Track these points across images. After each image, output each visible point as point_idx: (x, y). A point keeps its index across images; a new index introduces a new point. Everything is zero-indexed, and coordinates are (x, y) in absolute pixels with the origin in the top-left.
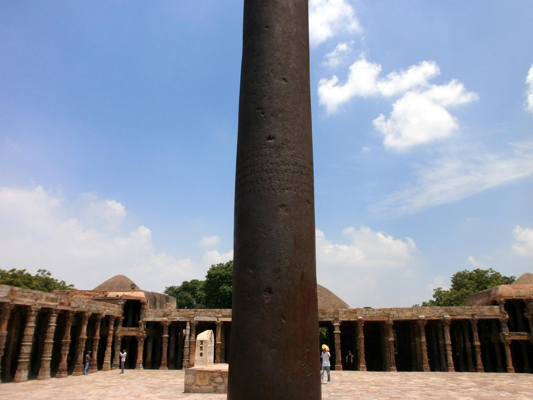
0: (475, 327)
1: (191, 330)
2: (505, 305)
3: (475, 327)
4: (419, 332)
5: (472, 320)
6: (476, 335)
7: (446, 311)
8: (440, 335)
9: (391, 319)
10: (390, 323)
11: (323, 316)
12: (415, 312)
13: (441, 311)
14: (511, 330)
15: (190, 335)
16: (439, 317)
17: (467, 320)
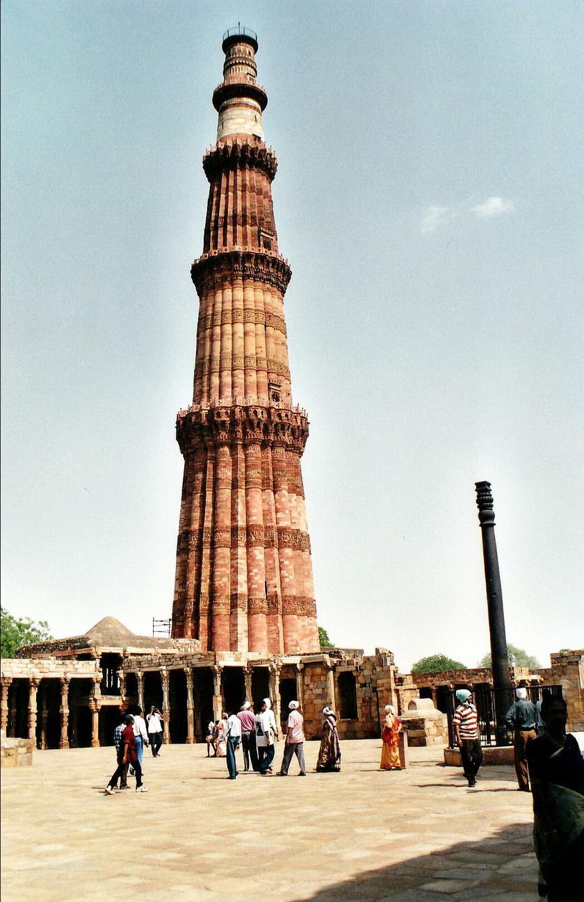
6: (65, 699)
17: (57, 680)
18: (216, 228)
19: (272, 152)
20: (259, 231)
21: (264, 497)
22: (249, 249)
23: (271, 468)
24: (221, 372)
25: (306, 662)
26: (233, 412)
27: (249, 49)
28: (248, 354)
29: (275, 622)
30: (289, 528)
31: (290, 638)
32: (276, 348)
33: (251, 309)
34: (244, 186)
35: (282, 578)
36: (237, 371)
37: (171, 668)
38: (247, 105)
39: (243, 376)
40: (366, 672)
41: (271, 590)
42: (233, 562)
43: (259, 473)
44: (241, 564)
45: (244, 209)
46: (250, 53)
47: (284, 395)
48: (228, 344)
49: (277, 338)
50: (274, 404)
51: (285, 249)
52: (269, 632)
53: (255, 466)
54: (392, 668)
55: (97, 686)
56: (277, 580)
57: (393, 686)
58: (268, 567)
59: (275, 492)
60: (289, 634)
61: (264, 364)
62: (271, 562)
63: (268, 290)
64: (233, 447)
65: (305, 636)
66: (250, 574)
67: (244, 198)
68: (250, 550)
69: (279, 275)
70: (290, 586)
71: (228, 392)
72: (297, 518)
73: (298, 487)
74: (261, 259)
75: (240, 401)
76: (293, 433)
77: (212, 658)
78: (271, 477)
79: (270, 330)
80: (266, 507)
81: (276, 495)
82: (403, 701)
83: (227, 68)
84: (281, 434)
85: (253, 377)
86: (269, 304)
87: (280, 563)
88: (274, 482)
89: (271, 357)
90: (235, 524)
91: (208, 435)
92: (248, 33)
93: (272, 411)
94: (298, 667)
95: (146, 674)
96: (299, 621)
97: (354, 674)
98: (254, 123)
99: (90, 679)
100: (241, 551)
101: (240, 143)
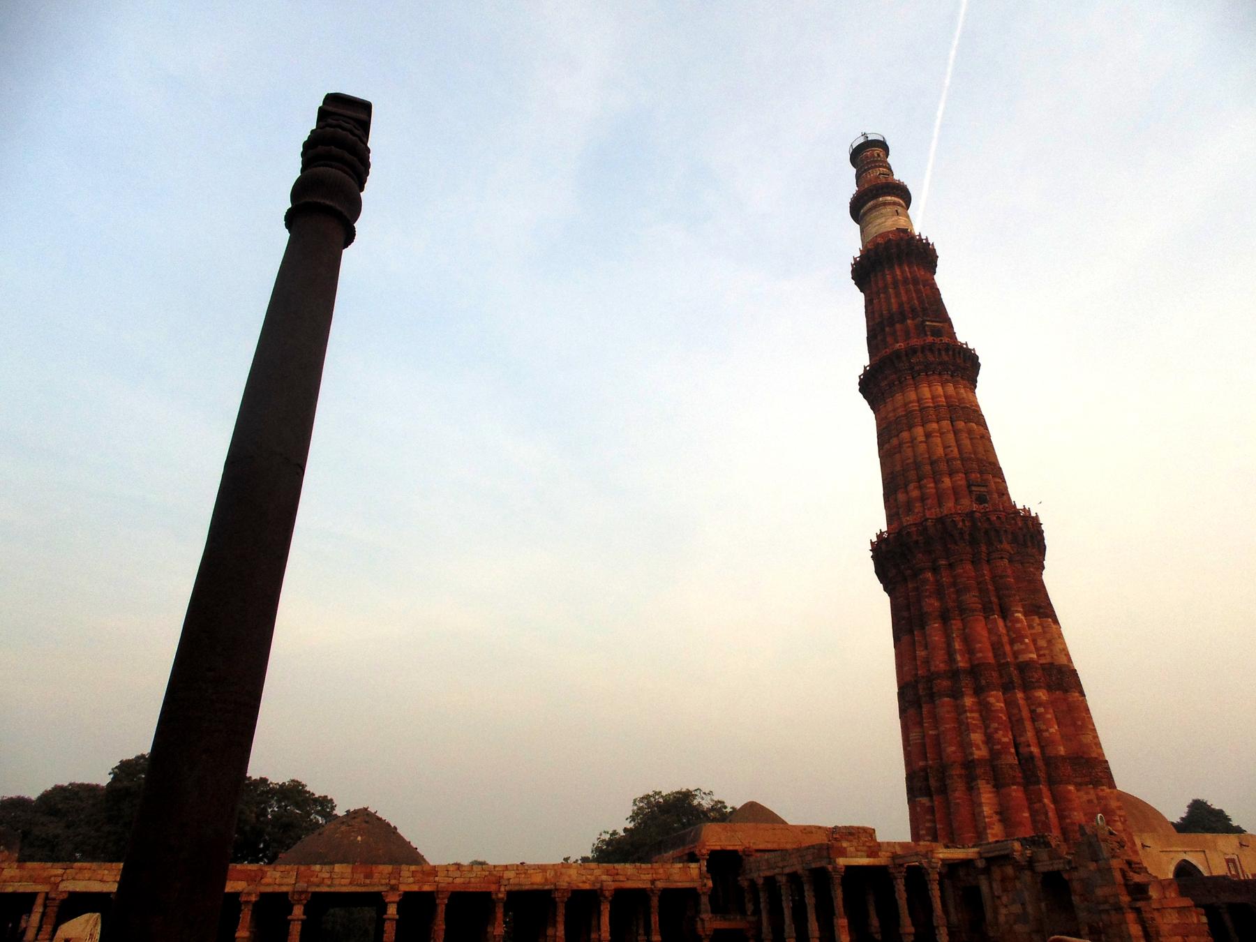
0: (655, 902)
1: (44, 914)
2: (708, 861)
3: (655, 902)
4: (555, 915)
5: (652, 890)
6: (655, 919)
7: (608, 873)
8: (594, 923)
9: (502, 889)
10: (500, 896)
11: (368, 881)
12: (550, 874)
13: (597, 872)
14: (715, 910)
15: (40, 929)
16: (593, 883)
19: (923, 237)
24: (906, 486)
25: (986, 855)
26: (926, 529)
27: (878, 150)
28: (935, 458)
32: (973, 445)
34: (895, 284)
35: (1038, 732)
37: (787, 870)
38: (885, 204)
39: (932, 485)
40: (1082, 873)
41: (1023, 750)
42: (963, 717)
44: (973, 718)
45: (901, 305)
47: (995, 496)
48: (908, 452)
49: (970, 432)
51: (964, 334)
52: (1033, 813)
54: (1115, 863)
55: (704, 900)
56: (1030, 734)
57: (1125, 899)
59: (1004, 618)
62: (1015, 711)
64: (935, 570)
67: (897, 295)
69: (965, 365)
71: (918, 506)
72: (1046, 648)
73: (1040, 607)
74: (931, 348)
77: (825, 853)
78: (994, 599)
79: (961, 425)
80: (994, 638)
82: (1158, 933)
83: (858, 177)
85: (947, 482)
86: (951, 397)
87: (1032, 712)
88: (1000, 606)
93: (977, 515)
94: (980, 864)
95: (766, 878)
96: (1079, 794)
97: (1065, 876)
99: (694, 889)
100: (968, 701)
101: (880, 240)
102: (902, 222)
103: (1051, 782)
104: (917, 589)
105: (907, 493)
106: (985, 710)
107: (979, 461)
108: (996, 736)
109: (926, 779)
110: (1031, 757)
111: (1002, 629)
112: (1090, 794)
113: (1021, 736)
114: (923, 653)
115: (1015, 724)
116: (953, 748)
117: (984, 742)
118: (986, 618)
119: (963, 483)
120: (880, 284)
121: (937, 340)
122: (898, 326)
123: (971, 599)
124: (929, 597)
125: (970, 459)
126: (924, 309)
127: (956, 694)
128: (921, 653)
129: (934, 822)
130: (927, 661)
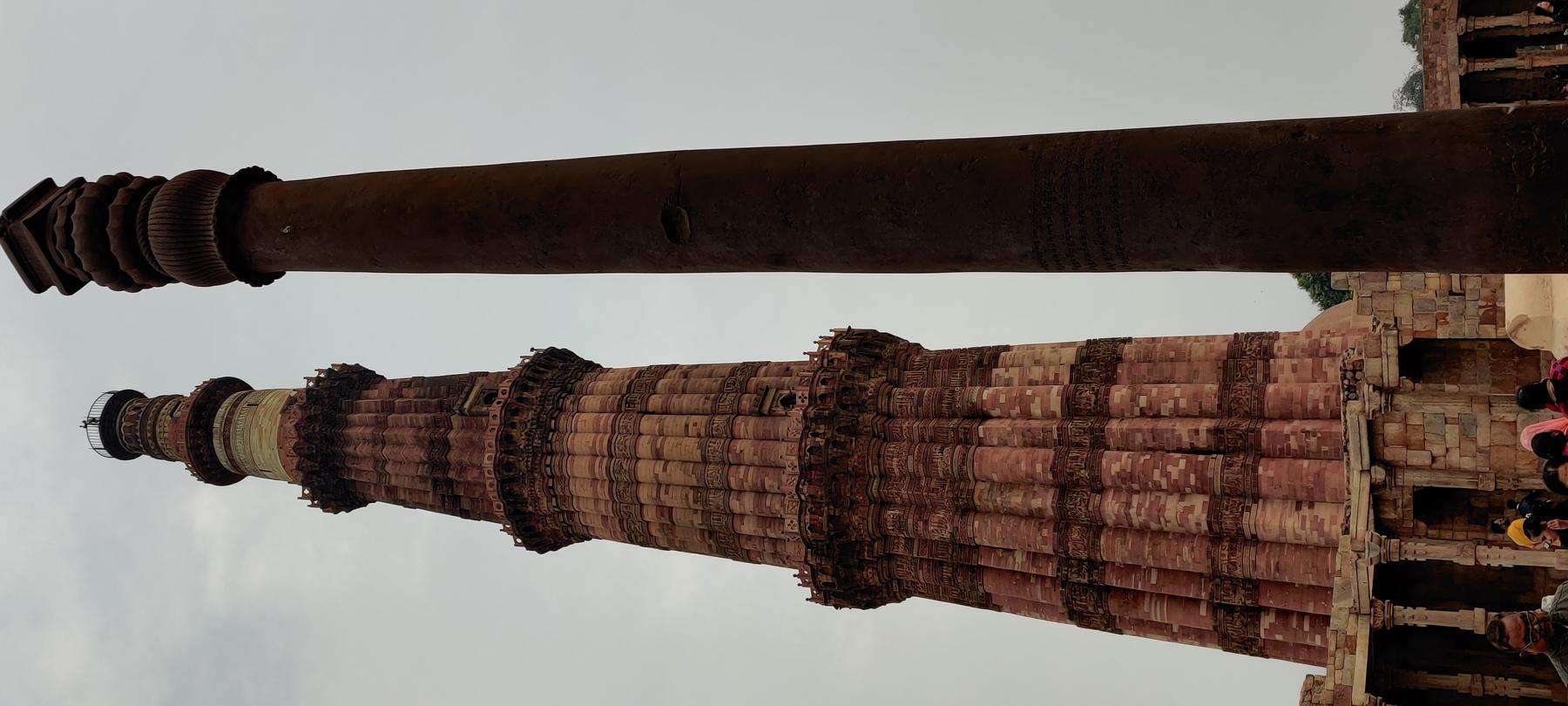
18: (457, 498)
20: (462, 413)
21: (995, 442)
22: (490, 438)
23: (933, 423)
27: (128, 408)
28: (697, 456)
29: (1273, 435)
30: (1066, 389)
31: (1321, 406)
33: (610, 441)
35: (1177, 414)
36: (732, 480)
38: (228, 422)
39: (742, 469)
41: (1203, 440)
42: (1136, 521)
43: (942, 451)
44: (1140, 506)
45: (419, 441)
46: (136, 408)
50: (797, 413)
53: (927, 461)
58: (1150, 444)
59: (987, 417)
60: (1309, 406)
61: (718, 420)
62: (1139, 438)
63: (576, 401)
64: (885, 504)
65: (1318, 374)
66: (1164, 486)
68: (1109, 483)
70: (1196, 397)
74: (510, 411)
75: (789, 480)
76: (866, 370)
79: (655, 402)
80: (1016, 440)
81: (993, 413)
83: (159, 454)
84: (864, 397)
85: (745, 447)
86: (604, 404)
87: (1143, 414)
89: (708, 406)
90: (1051, 513)
91: (860, 552)
92: (97, 414)
93: (811, 412)
98: (261, 410)
102: (277, 404)
103: (1262, 418)
104: (909, 540)
105: (742, 515)
106: (1129, 483)
107: (721, 391)
108: (1175, 476)
109: (1230, 610)
110: (1216, 431)
111: (1006, 424)
112: (1282, 366)
113: (1179, 439)
114: (1019, 558)
115: (1159, 447)
116: (1186, 549)
117: (1183, 495)
118: (980, 444)
119: (752, 421)
120: (367, 466)
121: (501, 397)
122: (453, 456)
123: (945, 459)
124: (926, 523)
125: (715, 400)
126: (440, 407)
127: (1096, 526)
128: (1019, 562)
129: (1302, 615)
130: (1034, 557)
